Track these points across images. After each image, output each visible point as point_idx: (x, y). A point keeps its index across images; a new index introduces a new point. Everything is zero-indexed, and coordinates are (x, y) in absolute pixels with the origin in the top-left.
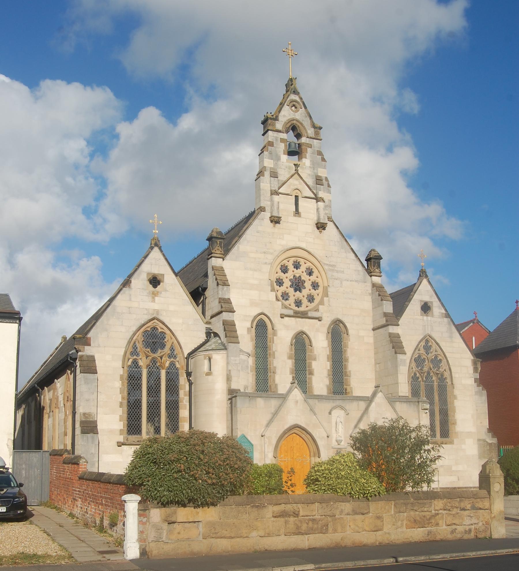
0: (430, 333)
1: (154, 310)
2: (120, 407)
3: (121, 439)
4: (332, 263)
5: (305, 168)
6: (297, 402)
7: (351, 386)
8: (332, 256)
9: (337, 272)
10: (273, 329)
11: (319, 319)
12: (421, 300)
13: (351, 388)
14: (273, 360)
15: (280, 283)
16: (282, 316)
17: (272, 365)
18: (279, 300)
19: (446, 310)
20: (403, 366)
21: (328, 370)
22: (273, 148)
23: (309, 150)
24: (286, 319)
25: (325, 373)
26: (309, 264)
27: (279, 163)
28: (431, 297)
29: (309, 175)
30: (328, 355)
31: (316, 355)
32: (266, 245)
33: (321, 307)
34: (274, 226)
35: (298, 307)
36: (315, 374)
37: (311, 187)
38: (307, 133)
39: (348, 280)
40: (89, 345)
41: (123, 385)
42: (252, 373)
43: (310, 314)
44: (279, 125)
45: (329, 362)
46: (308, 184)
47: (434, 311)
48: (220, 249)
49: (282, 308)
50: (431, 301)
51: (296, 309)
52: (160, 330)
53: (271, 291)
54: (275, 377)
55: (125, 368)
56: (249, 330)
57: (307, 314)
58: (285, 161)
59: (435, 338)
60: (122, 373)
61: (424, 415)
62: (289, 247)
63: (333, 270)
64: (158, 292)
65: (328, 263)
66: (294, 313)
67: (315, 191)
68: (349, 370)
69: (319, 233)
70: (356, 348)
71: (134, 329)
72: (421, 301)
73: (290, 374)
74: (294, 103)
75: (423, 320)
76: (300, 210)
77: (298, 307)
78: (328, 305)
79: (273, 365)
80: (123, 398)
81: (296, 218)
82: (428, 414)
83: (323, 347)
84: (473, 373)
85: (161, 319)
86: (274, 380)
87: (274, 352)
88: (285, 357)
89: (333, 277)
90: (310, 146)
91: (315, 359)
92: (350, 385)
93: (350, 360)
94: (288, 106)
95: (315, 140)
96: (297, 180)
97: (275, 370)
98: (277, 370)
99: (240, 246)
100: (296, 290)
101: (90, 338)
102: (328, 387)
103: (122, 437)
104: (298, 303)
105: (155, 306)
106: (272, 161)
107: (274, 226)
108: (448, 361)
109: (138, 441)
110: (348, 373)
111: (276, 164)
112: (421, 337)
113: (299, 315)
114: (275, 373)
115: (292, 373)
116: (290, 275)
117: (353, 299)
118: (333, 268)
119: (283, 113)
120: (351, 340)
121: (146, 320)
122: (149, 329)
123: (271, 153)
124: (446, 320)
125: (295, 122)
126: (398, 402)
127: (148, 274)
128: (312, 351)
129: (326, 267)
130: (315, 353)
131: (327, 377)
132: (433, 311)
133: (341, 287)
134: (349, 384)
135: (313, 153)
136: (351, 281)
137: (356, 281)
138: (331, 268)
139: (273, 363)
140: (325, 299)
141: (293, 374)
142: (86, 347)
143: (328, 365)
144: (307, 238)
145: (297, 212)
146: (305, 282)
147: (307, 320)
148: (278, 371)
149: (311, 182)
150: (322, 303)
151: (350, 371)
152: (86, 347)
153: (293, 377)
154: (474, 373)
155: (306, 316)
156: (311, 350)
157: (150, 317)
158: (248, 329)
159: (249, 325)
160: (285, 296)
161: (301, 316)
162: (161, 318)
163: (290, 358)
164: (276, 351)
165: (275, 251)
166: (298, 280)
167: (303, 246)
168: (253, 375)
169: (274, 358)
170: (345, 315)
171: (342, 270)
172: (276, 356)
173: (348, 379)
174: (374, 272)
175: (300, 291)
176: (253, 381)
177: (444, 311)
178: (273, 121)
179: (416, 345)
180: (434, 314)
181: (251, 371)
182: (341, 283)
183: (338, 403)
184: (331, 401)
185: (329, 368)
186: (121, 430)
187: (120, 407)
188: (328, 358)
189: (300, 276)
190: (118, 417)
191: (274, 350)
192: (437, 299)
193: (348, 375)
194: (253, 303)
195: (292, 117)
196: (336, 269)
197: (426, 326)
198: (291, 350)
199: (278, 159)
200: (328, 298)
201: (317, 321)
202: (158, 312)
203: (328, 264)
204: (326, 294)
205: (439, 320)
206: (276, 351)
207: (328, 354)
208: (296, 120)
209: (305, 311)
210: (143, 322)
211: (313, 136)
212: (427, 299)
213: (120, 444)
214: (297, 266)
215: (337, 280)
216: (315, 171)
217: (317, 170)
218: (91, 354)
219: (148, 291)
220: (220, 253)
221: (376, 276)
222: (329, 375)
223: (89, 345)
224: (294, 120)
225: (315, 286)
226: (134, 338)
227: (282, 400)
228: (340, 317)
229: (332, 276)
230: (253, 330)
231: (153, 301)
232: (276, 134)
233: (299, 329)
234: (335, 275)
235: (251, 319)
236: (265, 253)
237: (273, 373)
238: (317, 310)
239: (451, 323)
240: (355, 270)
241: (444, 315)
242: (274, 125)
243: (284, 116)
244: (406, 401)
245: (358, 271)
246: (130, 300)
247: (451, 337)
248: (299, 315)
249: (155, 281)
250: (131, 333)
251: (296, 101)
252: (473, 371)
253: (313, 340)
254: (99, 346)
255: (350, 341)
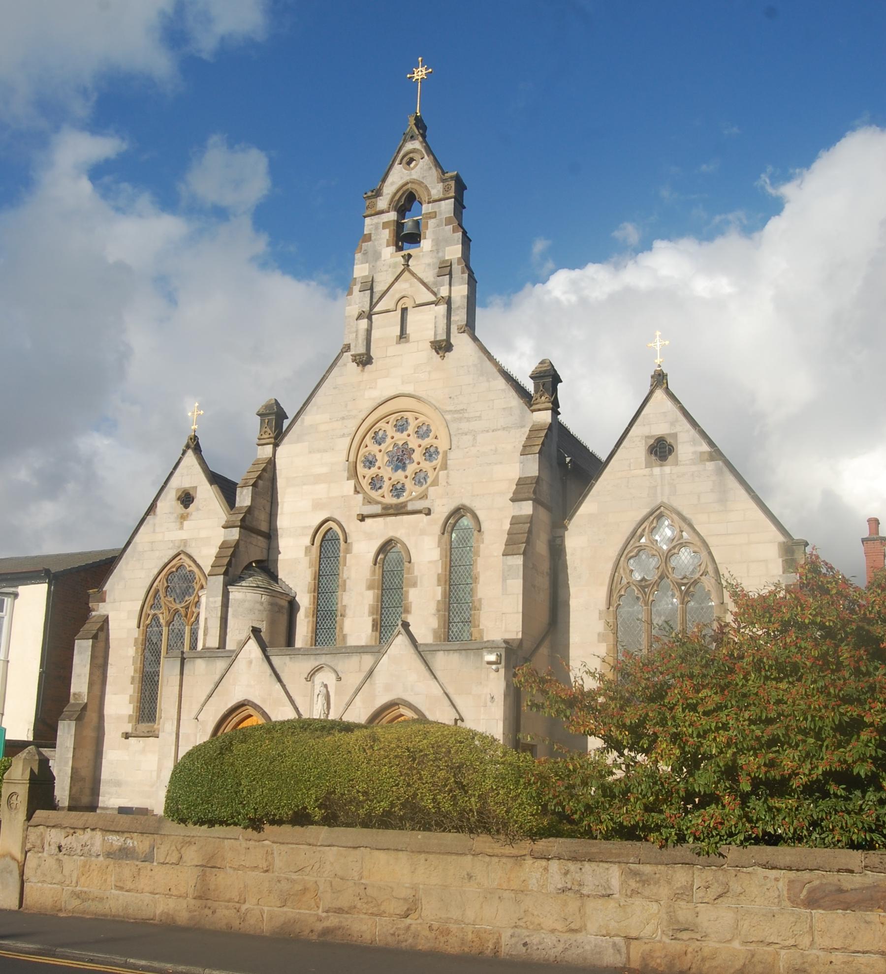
0: (666, 501)
1: (182, 540)
2: (132, 684)
3: (129, 728)
4: (459, 407)
5: (423, 255)
6: (250, 662)
7: (481, 627)
8: (461, 394)
9: (468, 420)
10: (346, 542)
11: (428, 512)
12: (647, 435)
13: (481, 632)
14: (342, 595)
15: (371, 463)
16: (362, 518)
17: (339, 602)
18: (358, 492)
19: (711, 443)
20: (513, 579)
21: (438, 601)
22: (369, 243)
23: (432, 223)
24: (368, 521)
25: (432, 607)
26: (422, 419)
27: (378, 263)
28: (673, 424)
29: (429, 265)
30: (438, 574)
31: (417, 577)
32: (346, 406)
33: (431, 489)
34: (363, 371)
35: (398, 498)
36: (413, 611)
37: (430, 285)
38: (429, 194)
39: (488, 431)
40: (104, 601)
41: (137, 652)
42: (306, 620)
43: (410, 507)
44: (382, 203)
45: (440, 587)
46: (426, 281)
47: (679, 452)
48: (269, 431)
49: (363, 504)
50: (672, 432)
51: (394, 501)
52: (188, 569)
53: (348, 480)
54: (343, 622)
55: (141, 628)
56: (307, 550)
57: (406, 506)
58: (389, 256)
59: (680, 509)
60: (137, 636)
61: (493, 675)
62: (383, 399)
63: (460, 420)
64: (188, 514)
65: (452, 408)
66: (383, 508)
67: (435, 290)
68: (479, 597)
69: (440, 359)
70: (496, 554)
71: (156, 571)
72: (647, 437)
73: (369, 616)
74: (411, 155)
75: (651, 475)
76: (410, 329)
77: (398, 496)
78: (446, 484)
79: (342, 603)
80: (135, 671)
81: (403, 346)
82: (502, 671)
83: (430, 562)
84: (781, 573)
85: (188, 552)
86: (342, 629)
87: (345, 581)
88: (363, 585)
89: (460, 431)
90: (433, 215)
91: (415, 585)
92: (479, 626)
93: (482, 579)
94: (400, 164)
95: (443, 202)
96: (406, 281)
97: (345, 611)
98: (347, 611)
99: (305, 417)
100: (396, 469)
101: (106, 592)
102: (435, 632)
103: (130, 725)
104: (397, 490)
105: (183, 535)
106: (368, 264)
107: (363, 371)
108: (710, 553)
109: (148, 732)
110: (476, 604)
111: (373, 268)
112: (645, 511)
113: (392, 511)
114: (344, 616)
115: (371, 613)
116: (387, 445)
117: (496, 464)
118: (461, 415)
119: (390, 179)
120: (485, 542)
121: (170, 557)
122: (174, 569)
123: (365, 254)
124: (710, 466)
125: (409, 186)
126: (442, 652)
127: (178, 490)
128: (410, 571)
129: (448, 417)
130: (416, 573)
131: (435, 615)
132: (677, 452)
133: (473, 446)
134: (477, 623)
135: (438, 225)
136: (493, 431)
137: (504, 429)
138: (456, 416)
139: (342, 598)
140: (442, 474)
141: (373, 614)
142: (100, 604)
143: (438, 593)
144: (416, 375)
145: (403, 335)
146: (414, 451)
147: (405, 517)
148: (349, 613)
149: (429, 276)
150: (435, 483)
151: (480, 600)
152: (101, 604)
153: (373, 620)
154: (783, 573)
155: (403, 510)
156: (409, 569)
157: (175, 552)
158: (306, 548)
159: (307, 541)
160: (376, 483)
161: (396, 512)
162: (189, 551)
163: (370, 587)
164: (348, 578)
165: (360, 412)
166: (403, 451)
167: (409, 389)
168: (308, 622)
169: (345, 591)
170: (478, 495)
171: (478, 414)
172: (347, 587)
173: (474, 614)
174: (537, 404)
175: (404, 468)
176: (307, 633)
177: (705, 448)
178: (373, 200)
179: (631, 529)
180: (679, 459)
181: (306, 616)
182: (475, 439)
183: (323, 660)
184: (312, 657)
185: (440, 598)
186: (130, 716)
187: (132, 684)
188: (439, 580)
189: (406, 443)
190: (127, 698)
191: (345, 576)
192: (688, 426)
193: (475, 607)
194: (317, 506)
195: (406, 179)
196: (466, 415)
197: (659, 488)
198: (373, 573)
199: (377, 256)
200: (445, 472)
201: (422, 516)
202: (185, 542)
203: (451, 411)
204: (445, 466)
205: (694, 468)
206: (348, 578)
207: (440, 571)
208: (410, 182)
209: (402, 503)
210: (166, 561)
211: (441, 196)
212: (661, 429)
213: (127, 736)
214: (401, 427)
215: (466, 434)
216: (440, 254)
217: (444, 252)
218: (105, 613)
219: (175, 515)
220: (268, 436)
221: (539, 410)
222: (438, 611)
223: (104, 601)
224: (407, 183)
225: (430, 453)
226: (155, 585)
227: (229, 661)
228: (467, 502)
229: (458, 429)
230: (315, 549)
231: (181, 528)
232: (376, 219)
233: (390, 534)
234: (464, 426)
235: (312, 531)
236: (343, 418)
237: (341, 616)
238: (424, 496)
239: (725, 469)
240: (504, 409)
241: (706, 456)
242: (374, 205)
243: (392, 183)
244: (456, 648)
245: (511, 408)
246: (154, 531)
247: (723, 499)
248: (392, 511)
249: (186, 499)
250: (152, 578)
251: (414, 151)
252: (783, 567)
253: (412, 552)
254: (114, 602)
255: (483, 543)
